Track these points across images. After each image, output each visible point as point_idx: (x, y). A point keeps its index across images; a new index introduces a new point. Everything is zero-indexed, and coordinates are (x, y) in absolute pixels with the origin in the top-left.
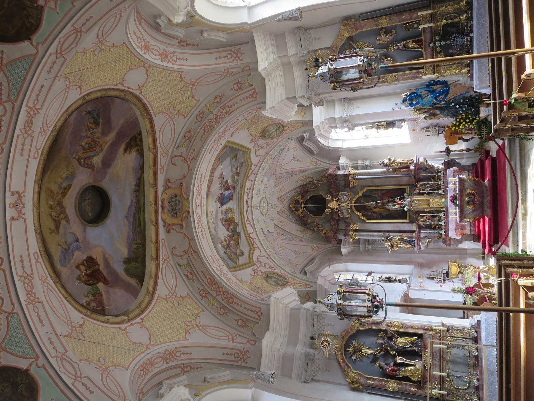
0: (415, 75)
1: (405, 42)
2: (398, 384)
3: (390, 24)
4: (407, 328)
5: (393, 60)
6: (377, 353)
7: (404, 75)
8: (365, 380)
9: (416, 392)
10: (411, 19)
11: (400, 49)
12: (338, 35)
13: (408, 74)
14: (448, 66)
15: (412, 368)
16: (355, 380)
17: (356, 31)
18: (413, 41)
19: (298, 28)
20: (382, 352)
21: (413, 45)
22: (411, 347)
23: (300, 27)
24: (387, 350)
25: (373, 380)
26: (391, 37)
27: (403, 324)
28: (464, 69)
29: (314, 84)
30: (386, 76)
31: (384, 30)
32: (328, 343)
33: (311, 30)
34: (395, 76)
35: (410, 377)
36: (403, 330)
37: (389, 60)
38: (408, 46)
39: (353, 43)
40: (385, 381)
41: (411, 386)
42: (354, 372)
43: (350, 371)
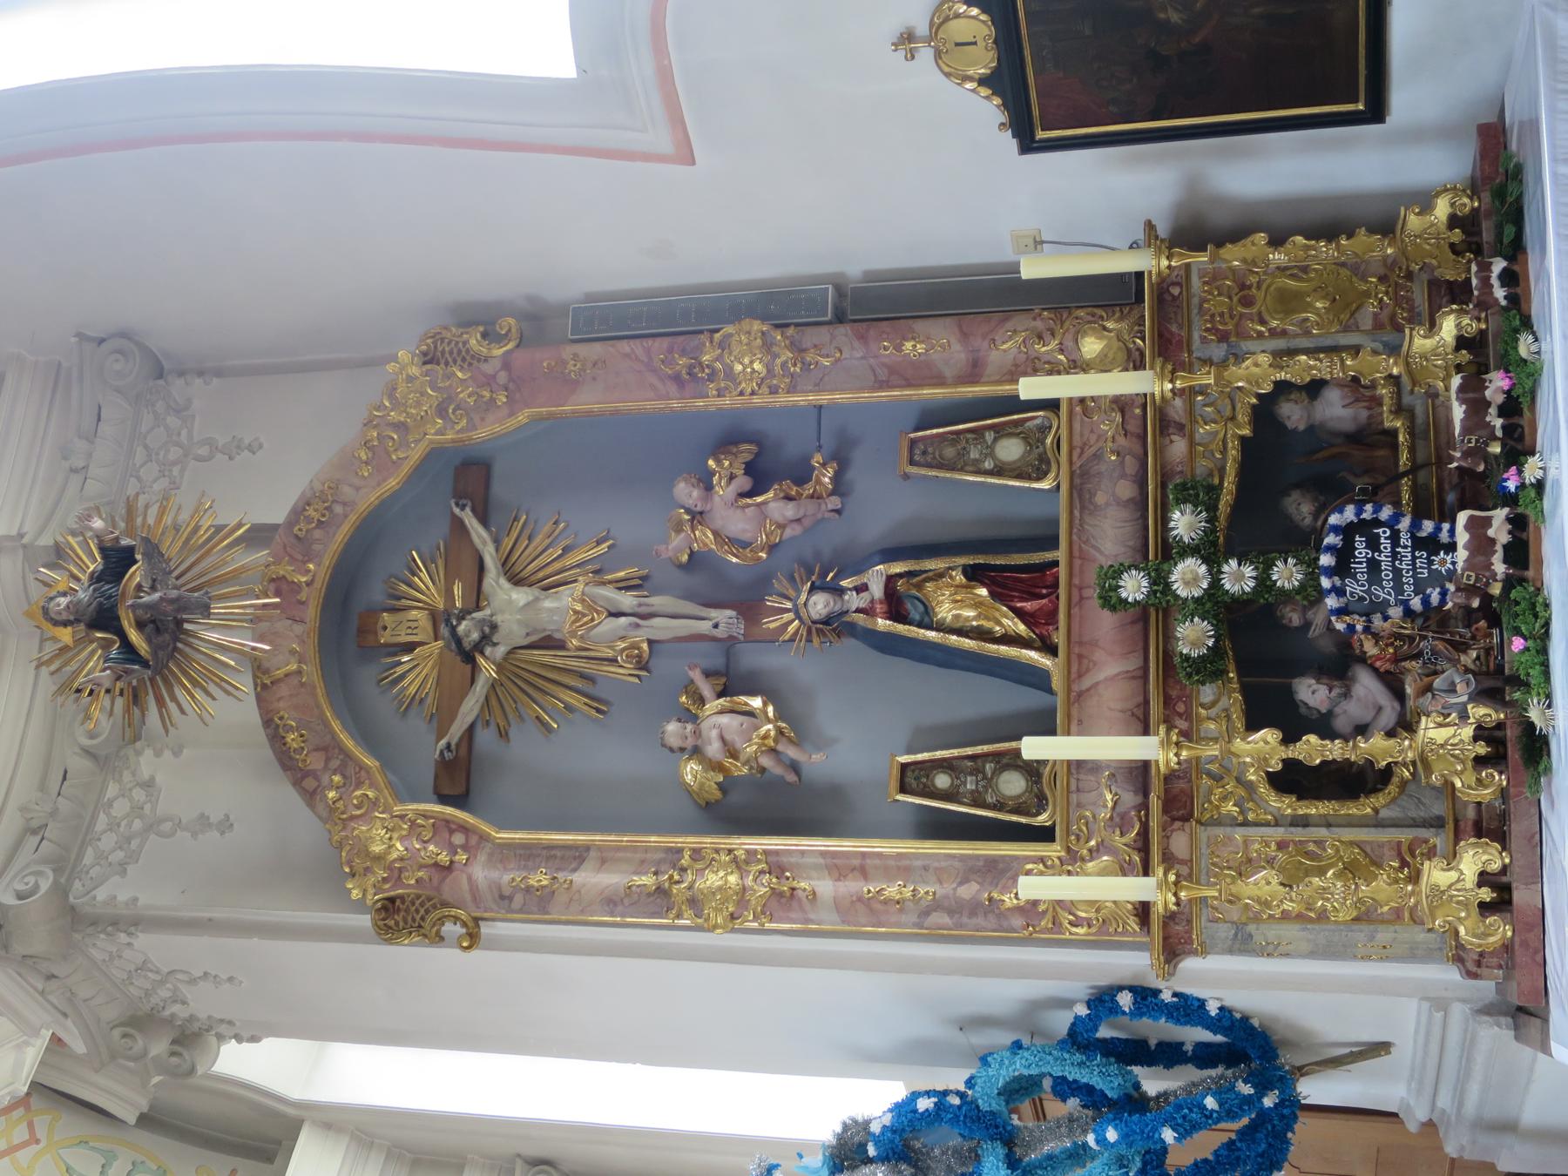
0: (968, 891)
1: (898, 568)
3: (791, 390)
5: (780, 715)
7: (861, 867)
10: (973, 373)
11: (851, 630)
12: (368, 424)
13: (901, 868)
14: (1279, 833)
17: (513, 406)
18: (975, 574)
19: (101, 341)
21: (978, 604)
23: (124, 335)
26: (790, 510)
28: (1452, 858)
29: (102, 821)
30: (697, 854)
31: (747, 451)
33: (198, 381)
34: (776, 866)
37: (750, 714)
38: (928, 610)
39: (484, 521)
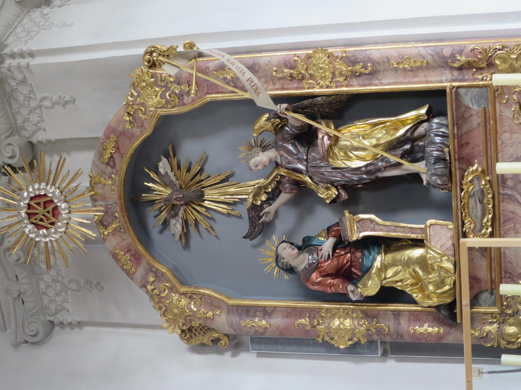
2: (366, 315)
4: (373, 74)
6: (264, 198)
8: (235, 319)
9: (439, 337)
15: (417, 252)
16: (196, 324)
20: (284, 197)
22: (398, 165)
24: (298, 185)
25: (266, 312)
27: (352, 61)
32: (50, 208)
35: (407, 290)
36: (357, 88)
40: (313, 313)
41: (415, 317)
42: (184, 294)
43: (172, 289)
